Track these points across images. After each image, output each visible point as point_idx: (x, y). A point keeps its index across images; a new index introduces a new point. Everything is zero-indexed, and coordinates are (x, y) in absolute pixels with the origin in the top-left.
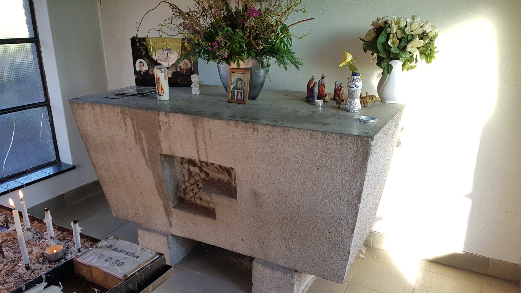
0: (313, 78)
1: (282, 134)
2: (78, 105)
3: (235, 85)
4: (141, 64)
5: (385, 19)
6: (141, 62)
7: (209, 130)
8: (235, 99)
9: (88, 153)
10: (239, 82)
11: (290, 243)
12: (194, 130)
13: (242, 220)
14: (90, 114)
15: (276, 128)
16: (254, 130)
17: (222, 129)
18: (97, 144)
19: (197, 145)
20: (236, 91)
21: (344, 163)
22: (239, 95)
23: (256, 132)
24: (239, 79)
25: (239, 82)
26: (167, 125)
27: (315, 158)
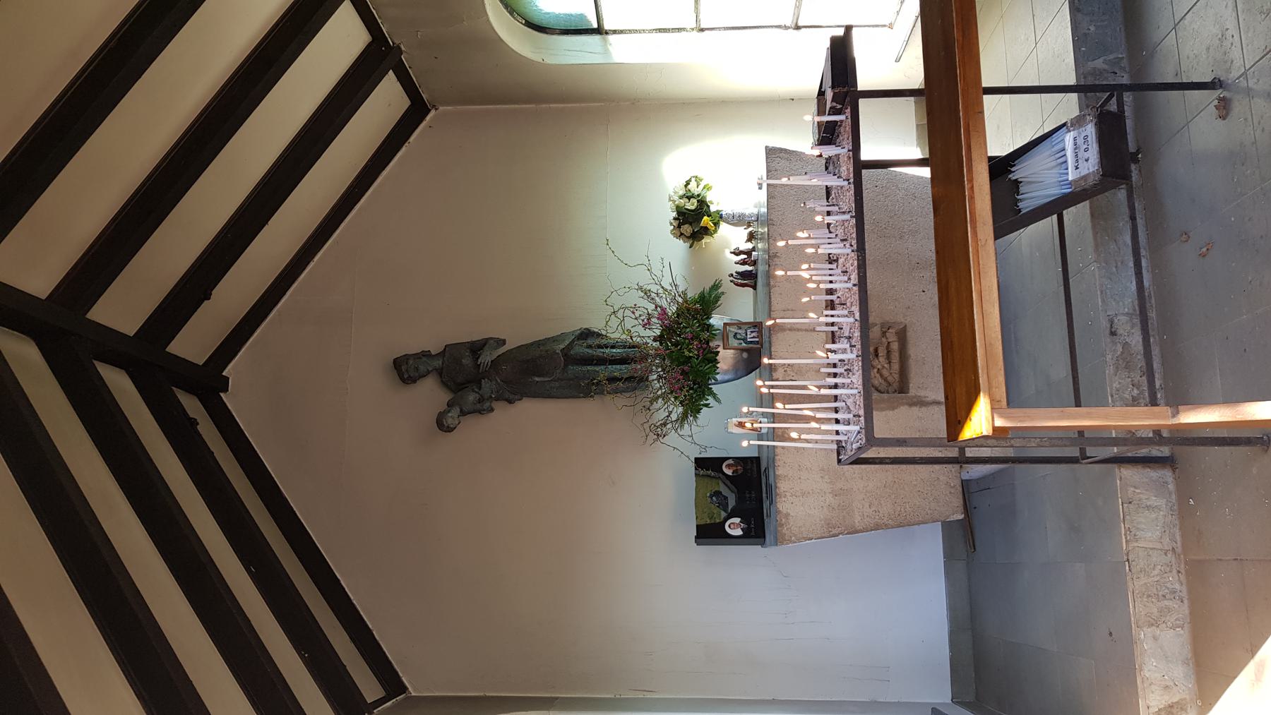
0: (731, 281)
1: (774, 227)
2: (783, 525)
3: (742, 341)
4: (732, 526)
5: (672, 221)
6: (729, 526)
7: (784, 311)
8: (757, 340)
9: (857, 532)
10: (739, 336)
11: (905, 230)
12: (788, 332)
13: (894, 287)
14: (792, 503)
15: (770, 233)
16: (775, 256)
17: (781, 294)
18: (839, 506)
19: (806, 330)
20: (749, 340)
21: (794, 168)
22: (754, 334)
23: (778, 254)
24: (735, 336)
25: (739, 336)
26: (788, 369)
27: (794, 195)
